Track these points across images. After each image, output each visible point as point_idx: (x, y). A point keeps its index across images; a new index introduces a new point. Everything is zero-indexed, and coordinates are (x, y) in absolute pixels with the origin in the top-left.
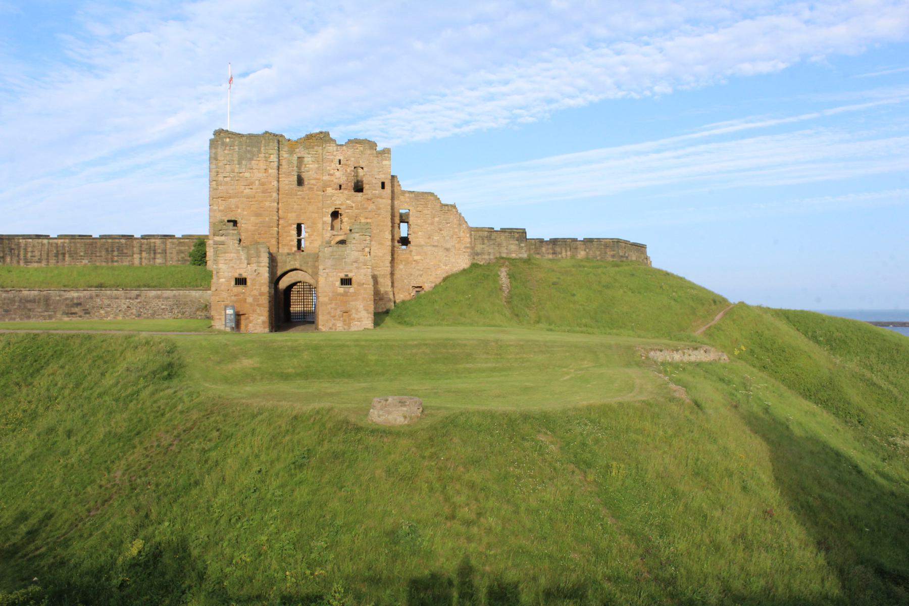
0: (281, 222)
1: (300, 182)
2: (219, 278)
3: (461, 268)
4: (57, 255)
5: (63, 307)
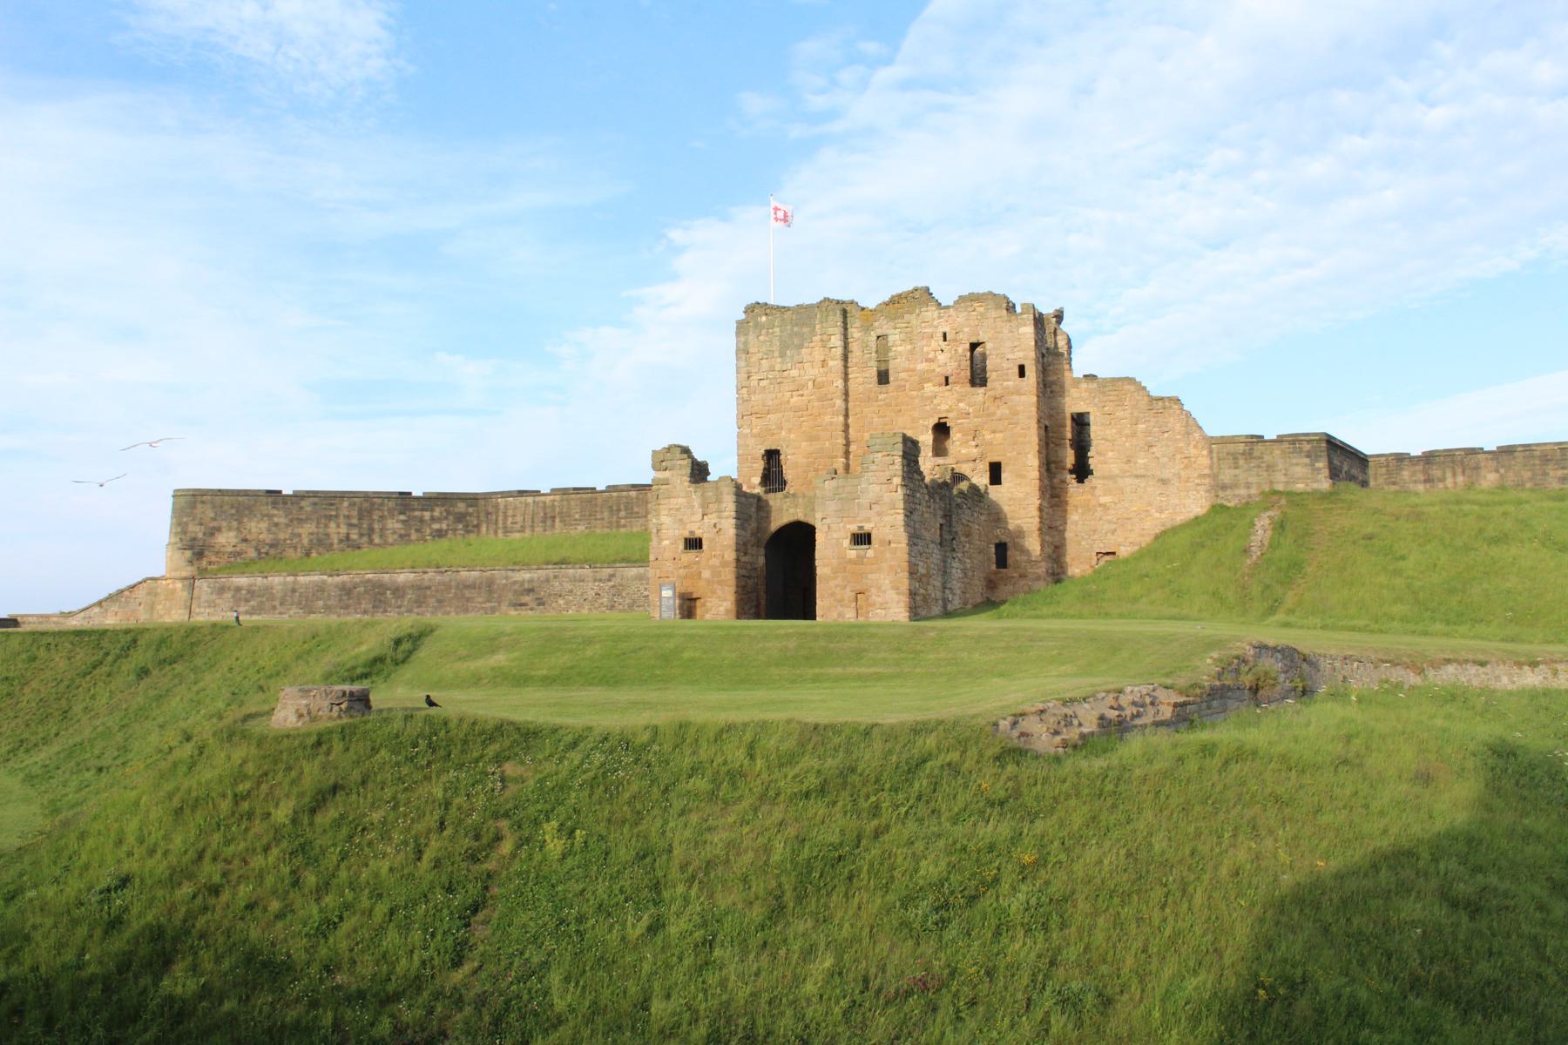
0: (853, 448)
1: (883, 377)
2: (660, 541)
3: (1192, 516)
4: (544, 522)
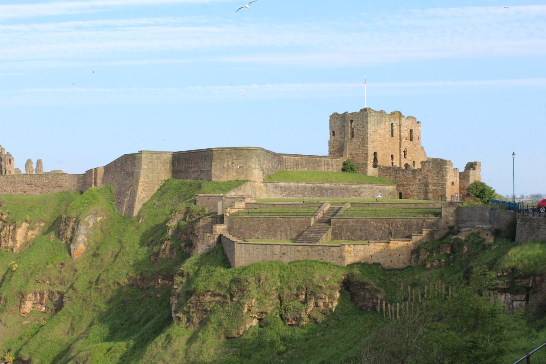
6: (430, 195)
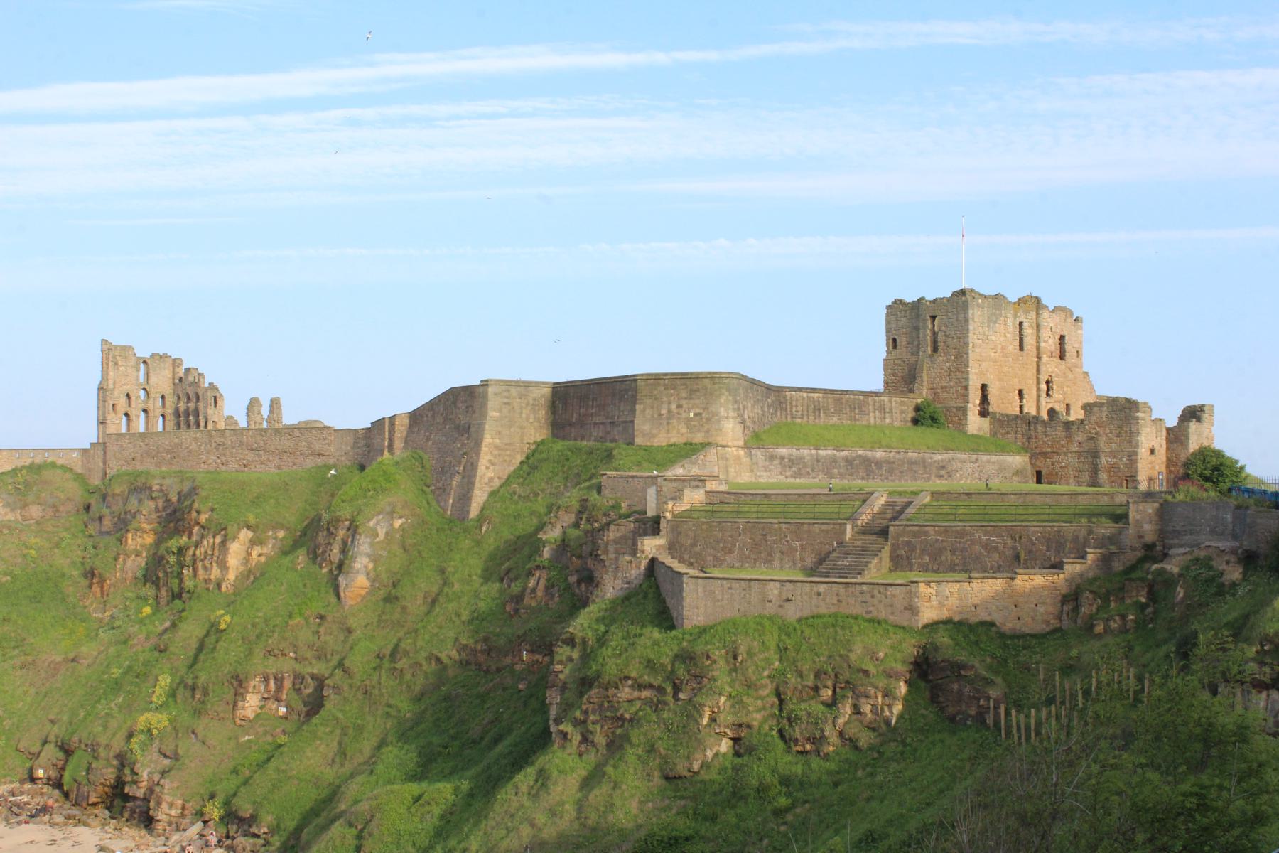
5: (934, 470)
6: (1103, 476)
